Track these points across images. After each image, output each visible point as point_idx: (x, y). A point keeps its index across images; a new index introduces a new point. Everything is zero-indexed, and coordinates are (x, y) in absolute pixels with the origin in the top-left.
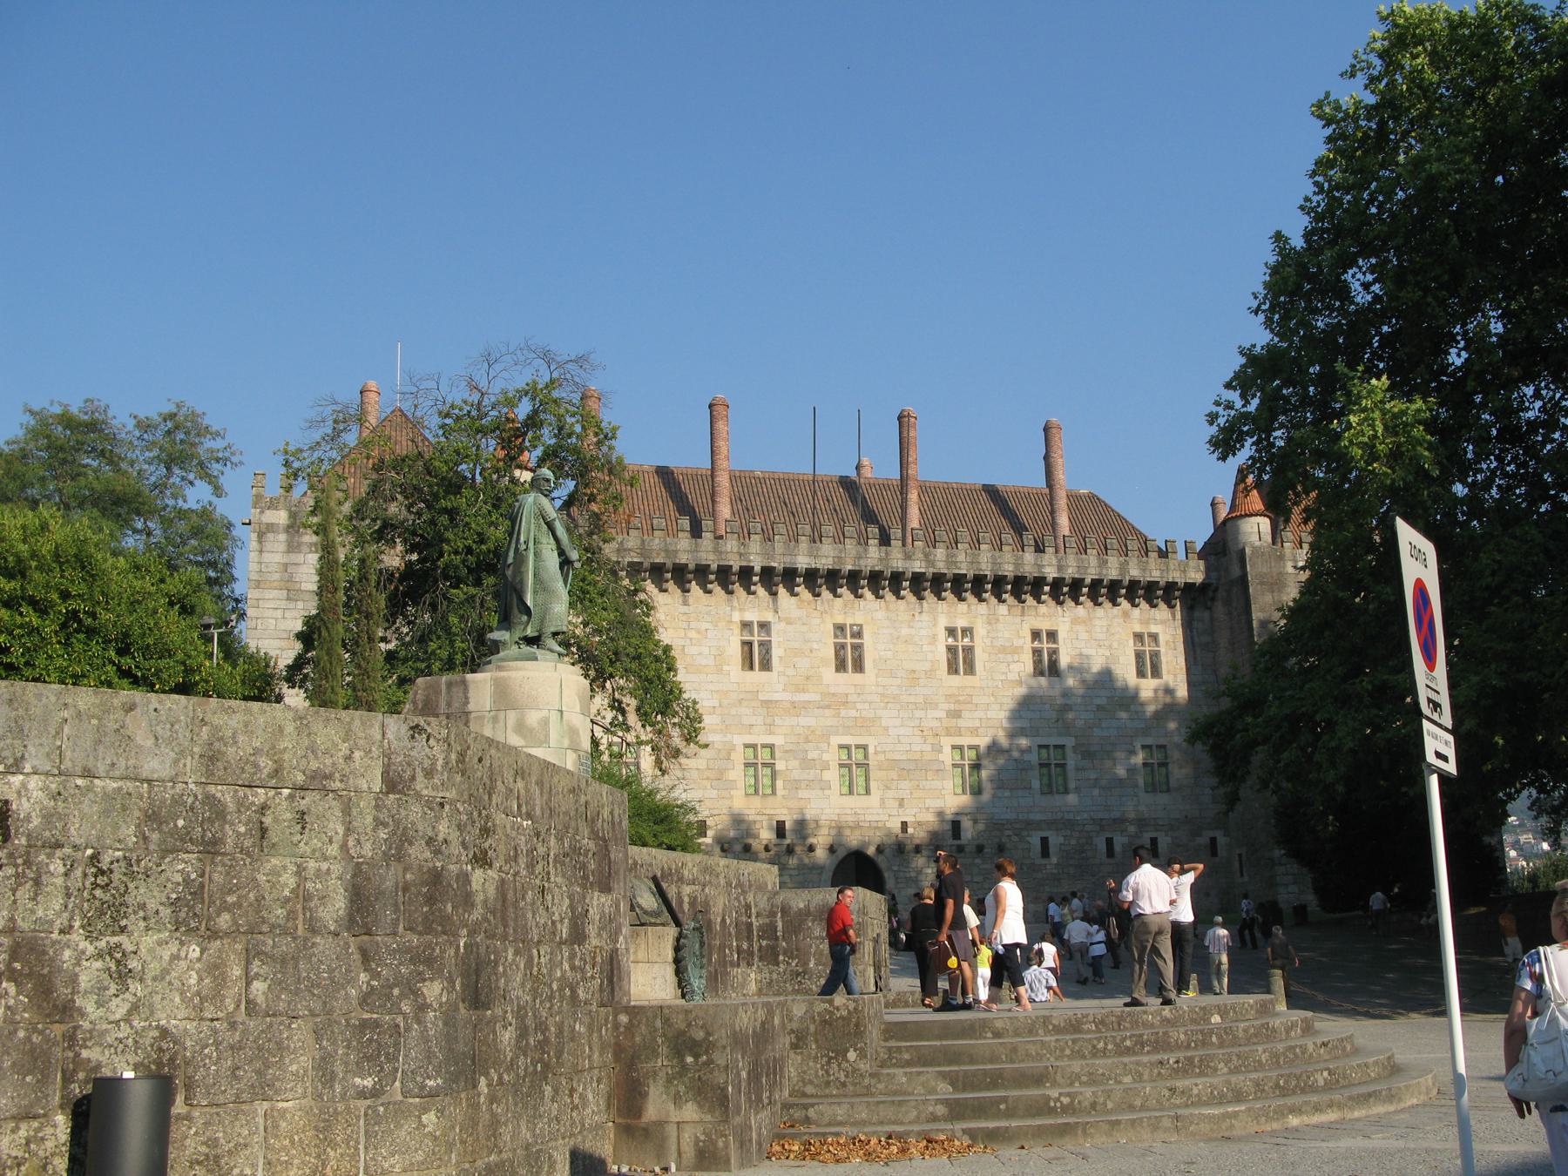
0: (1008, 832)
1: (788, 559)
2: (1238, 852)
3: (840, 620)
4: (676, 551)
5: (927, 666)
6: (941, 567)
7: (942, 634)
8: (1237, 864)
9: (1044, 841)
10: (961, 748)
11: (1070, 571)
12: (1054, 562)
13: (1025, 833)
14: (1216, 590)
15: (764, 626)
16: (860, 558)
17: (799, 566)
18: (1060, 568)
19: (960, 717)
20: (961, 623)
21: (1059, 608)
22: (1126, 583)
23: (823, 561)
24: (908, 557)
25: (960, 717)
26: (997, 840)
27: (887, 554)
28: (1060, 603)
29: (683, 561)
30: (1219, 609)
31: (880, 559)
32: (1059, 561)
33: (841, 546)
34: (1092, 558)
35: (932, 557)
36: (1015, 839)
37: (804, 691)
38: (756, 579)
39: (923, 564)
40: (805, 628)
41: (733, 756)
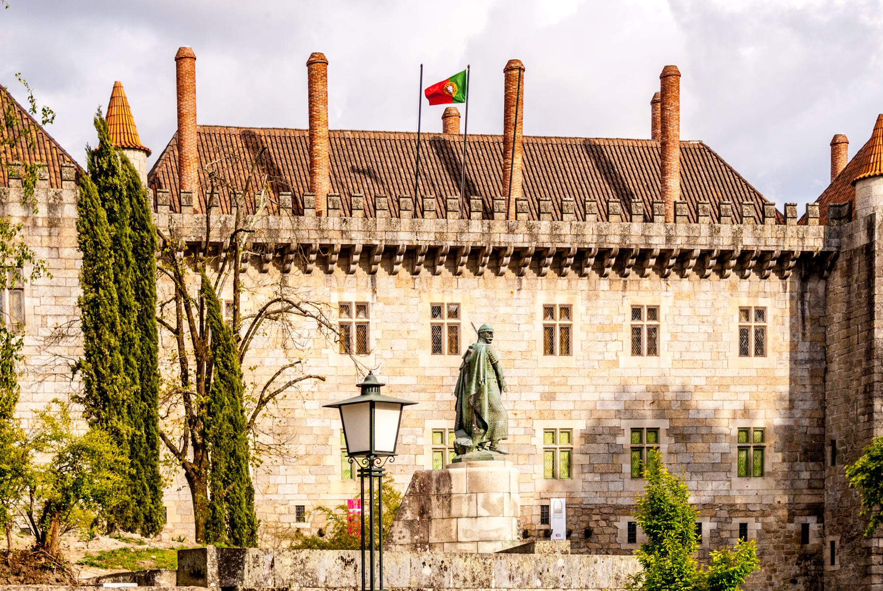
0: (595, 517)
1: (389, 236)
2: (831, 538)
3: (437, 299)
4: (278, 231)
5: (523, 346)
6: (544, 240)
7: (540, 312)
8: (827, 553)
9: (632, 527)
10: (553, 432)
11: (679, 241)
12: (663, 232)
13: (612, 518)
14: (837, 256)
15: (362, 307)
16: (462, 233)
17: (400, 243)
18: (669, 239)
19: (554, 399)
20: (560, 300)
21: (663, 281)
22: (737, 254)
23: (425, 237)
24: (511, 231)
25: (554, 399)
26: (584, 525)
27: (489, 228)
28: (665, 277)
29: (285, 241)
30: (837, 281)
31: (483, 234)
32: (668, 231)
33: (443, 221)
34: (704, 226)
35: (535, 231)
36: (603, 523)
37: (400, 374)
38: (356, 258)
39: (527, 238)
40: (402, 309)
41: (331, 441)
